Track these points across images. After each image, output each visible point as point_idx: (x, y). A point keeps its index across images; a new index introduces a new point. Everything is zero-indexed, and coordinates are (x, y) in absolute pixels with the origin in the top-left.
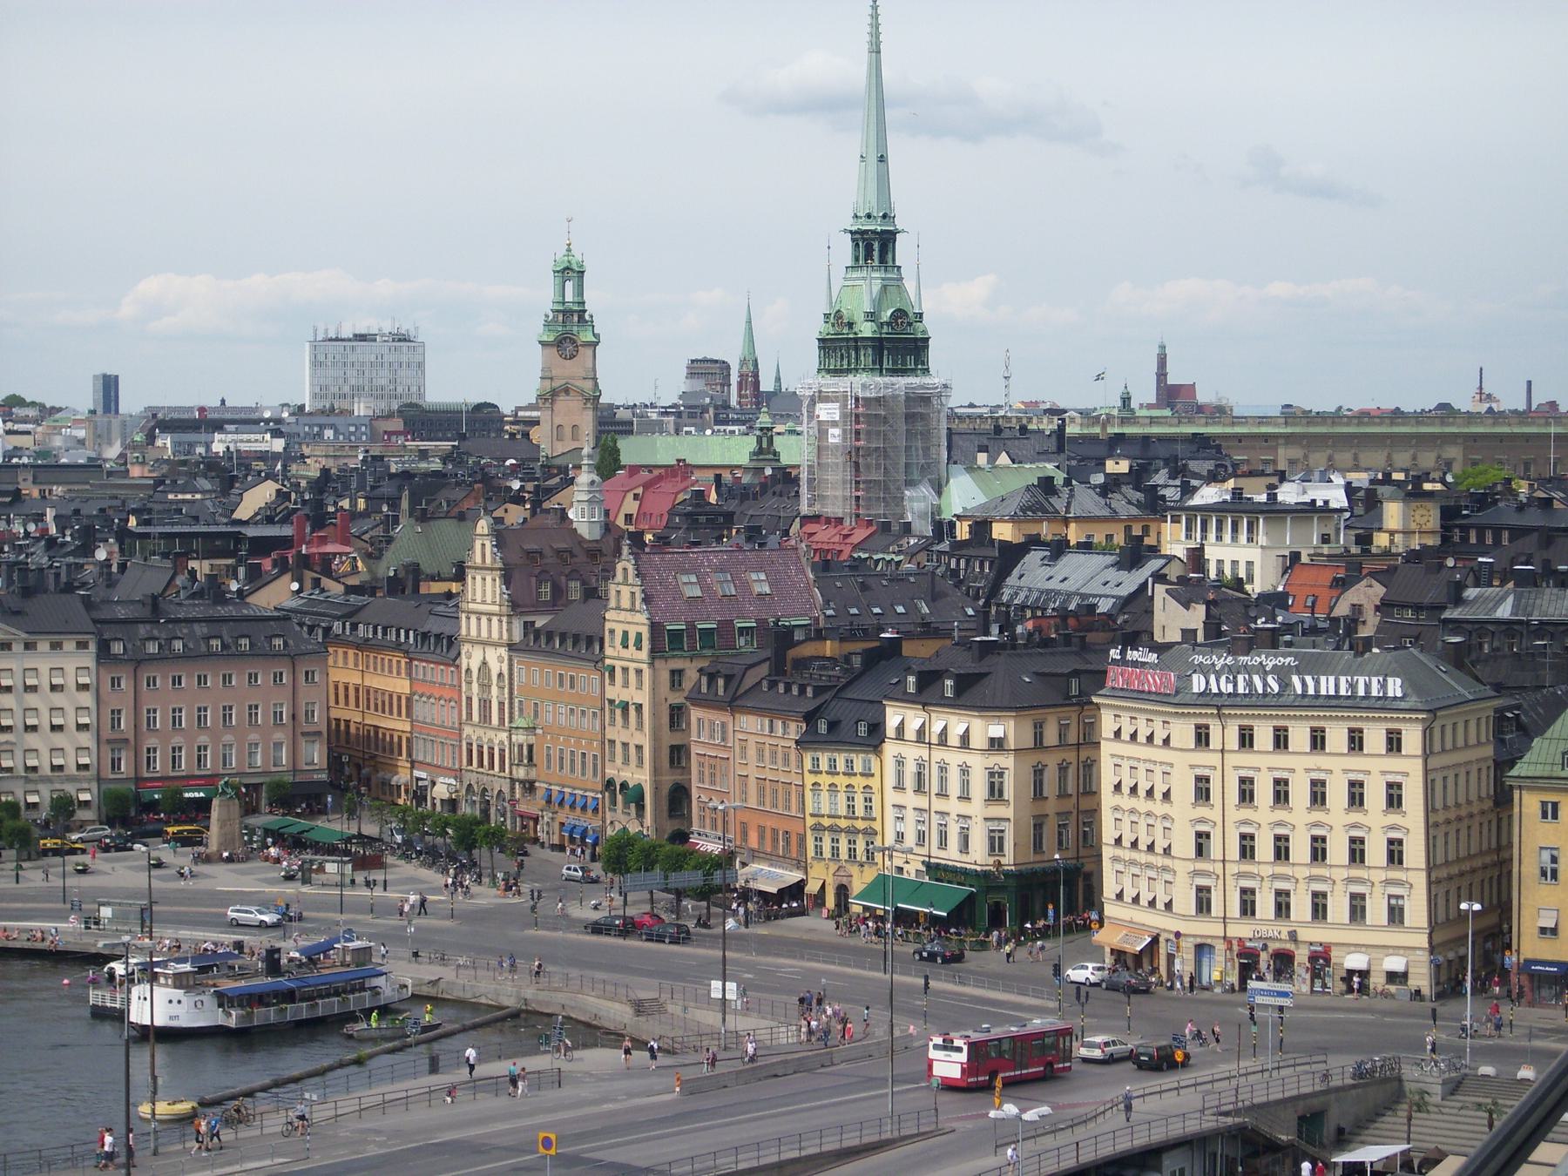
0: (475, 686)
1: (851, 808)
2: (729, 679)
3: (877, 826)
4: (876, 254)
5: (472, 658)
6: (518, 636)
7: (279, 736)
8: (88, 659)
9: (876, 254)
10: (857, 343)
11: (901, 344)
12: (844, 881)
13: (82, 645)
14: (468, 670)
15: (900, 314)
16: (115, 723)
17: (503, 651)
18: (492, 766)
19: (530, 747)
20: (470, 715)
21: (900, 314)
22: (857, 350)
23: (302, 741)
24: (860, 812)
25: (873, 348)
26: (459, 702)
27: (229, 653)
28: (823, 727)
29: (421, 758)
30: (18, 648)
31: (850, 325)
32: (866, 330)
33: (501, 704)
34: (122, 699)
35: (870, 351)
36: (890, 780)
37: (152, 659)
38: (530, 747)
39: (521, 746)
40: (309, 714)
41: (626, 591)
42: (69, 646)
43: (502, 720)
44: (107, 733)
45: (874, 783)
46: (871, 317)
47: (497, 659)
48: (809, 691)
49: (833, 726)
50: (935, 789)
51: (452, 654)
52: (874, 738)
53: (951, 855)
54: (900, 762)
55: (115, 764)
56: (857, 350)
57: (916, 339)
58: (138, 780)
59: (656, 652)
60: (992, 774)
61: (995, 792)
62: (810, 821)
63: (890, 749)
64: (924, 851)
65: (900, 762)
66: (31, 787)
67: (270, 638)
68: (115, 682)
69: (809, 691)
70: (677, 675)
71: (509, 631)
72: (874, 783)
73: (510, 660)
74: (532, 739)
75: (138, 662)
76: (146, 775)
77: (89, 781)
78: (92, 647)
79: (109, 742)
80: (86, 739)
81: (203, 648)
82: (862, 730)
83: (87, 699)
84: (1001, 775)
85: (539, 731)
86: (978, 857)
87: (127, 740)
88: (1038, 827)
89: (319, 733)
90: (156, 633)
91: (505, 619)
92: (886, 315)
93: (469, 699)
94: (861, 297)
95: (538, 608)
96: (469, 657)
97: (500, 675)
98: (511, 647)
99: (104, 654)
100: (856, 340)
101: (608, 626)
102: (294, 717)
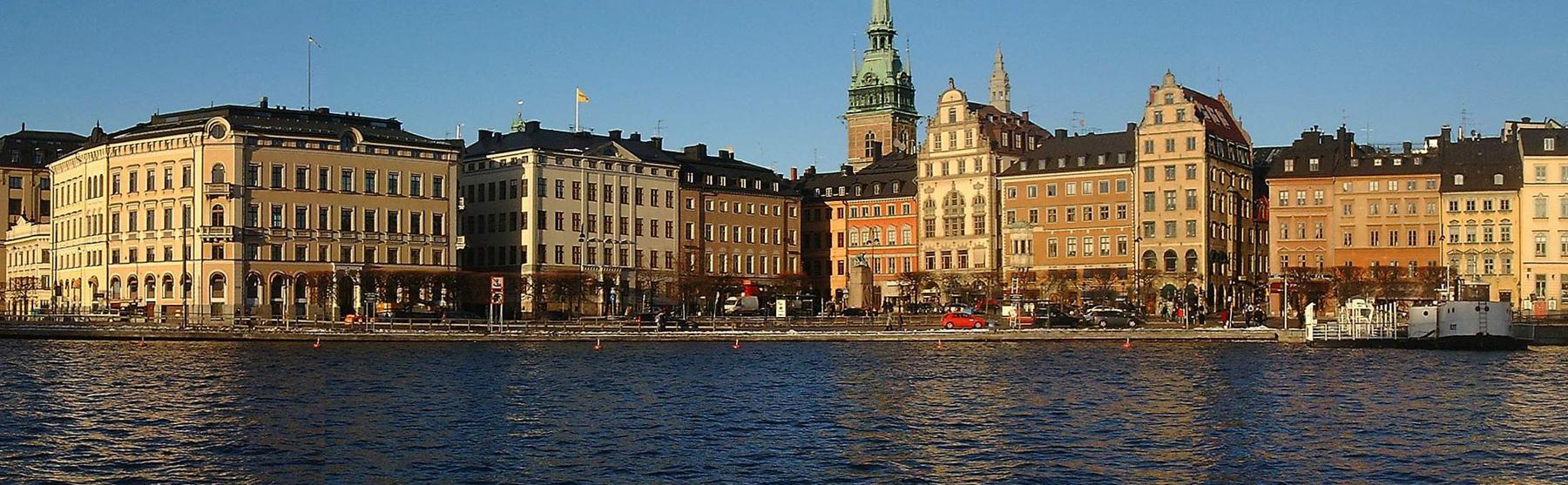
0: (939, 213)
1: (1489, 239)
3: (1514, 248)
7: (776, 252)
14: (930, 204)
17: (984, 181)
20: (930, 233)
24: (1497, 238)
28: (1459, 180)
42: (662, 172)
43: (979, 231)
45: (1512, 217)
52: (1515, 182)
54: (1541, 201)
59: (1209, 155)
65: (1541, 201)
72: (1512, 217)
82: (1499, 179)
91: (985, 159)
96: (930, 191)
97: (978, 200)
99: (682, 182)
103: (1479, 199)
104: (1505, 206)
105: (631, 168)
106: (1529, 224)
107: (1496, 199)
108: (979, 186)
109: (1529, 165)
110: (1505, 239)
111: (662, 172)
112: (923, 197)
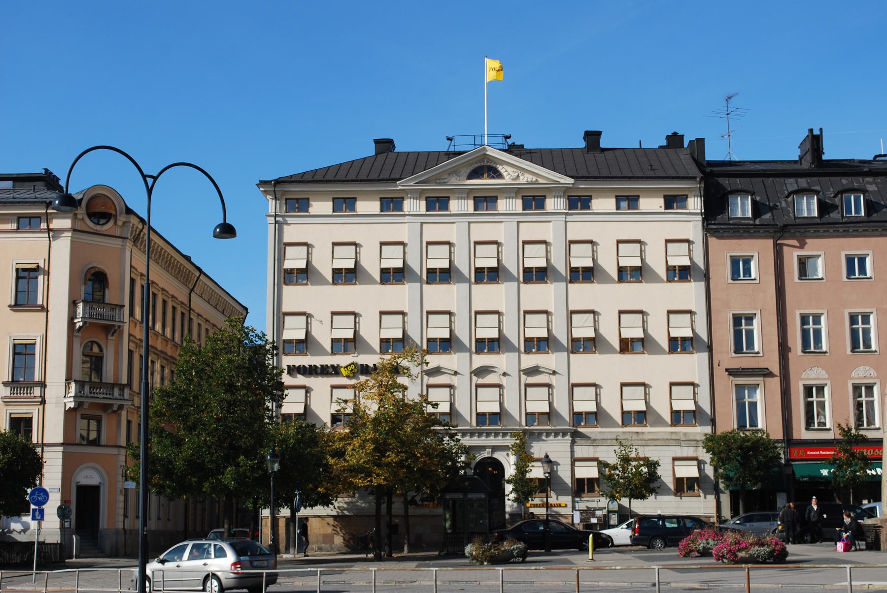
16: (741, 342)
30: (553, 204)
44: (726, 356)
58: (789, 440)
66: (582, 451)
68: (739, 267)
76: (801, 433)
78: (695, 204)
79: (732, 372)
80: (693, 365)
83: (690, 294)
87: (766, 373)
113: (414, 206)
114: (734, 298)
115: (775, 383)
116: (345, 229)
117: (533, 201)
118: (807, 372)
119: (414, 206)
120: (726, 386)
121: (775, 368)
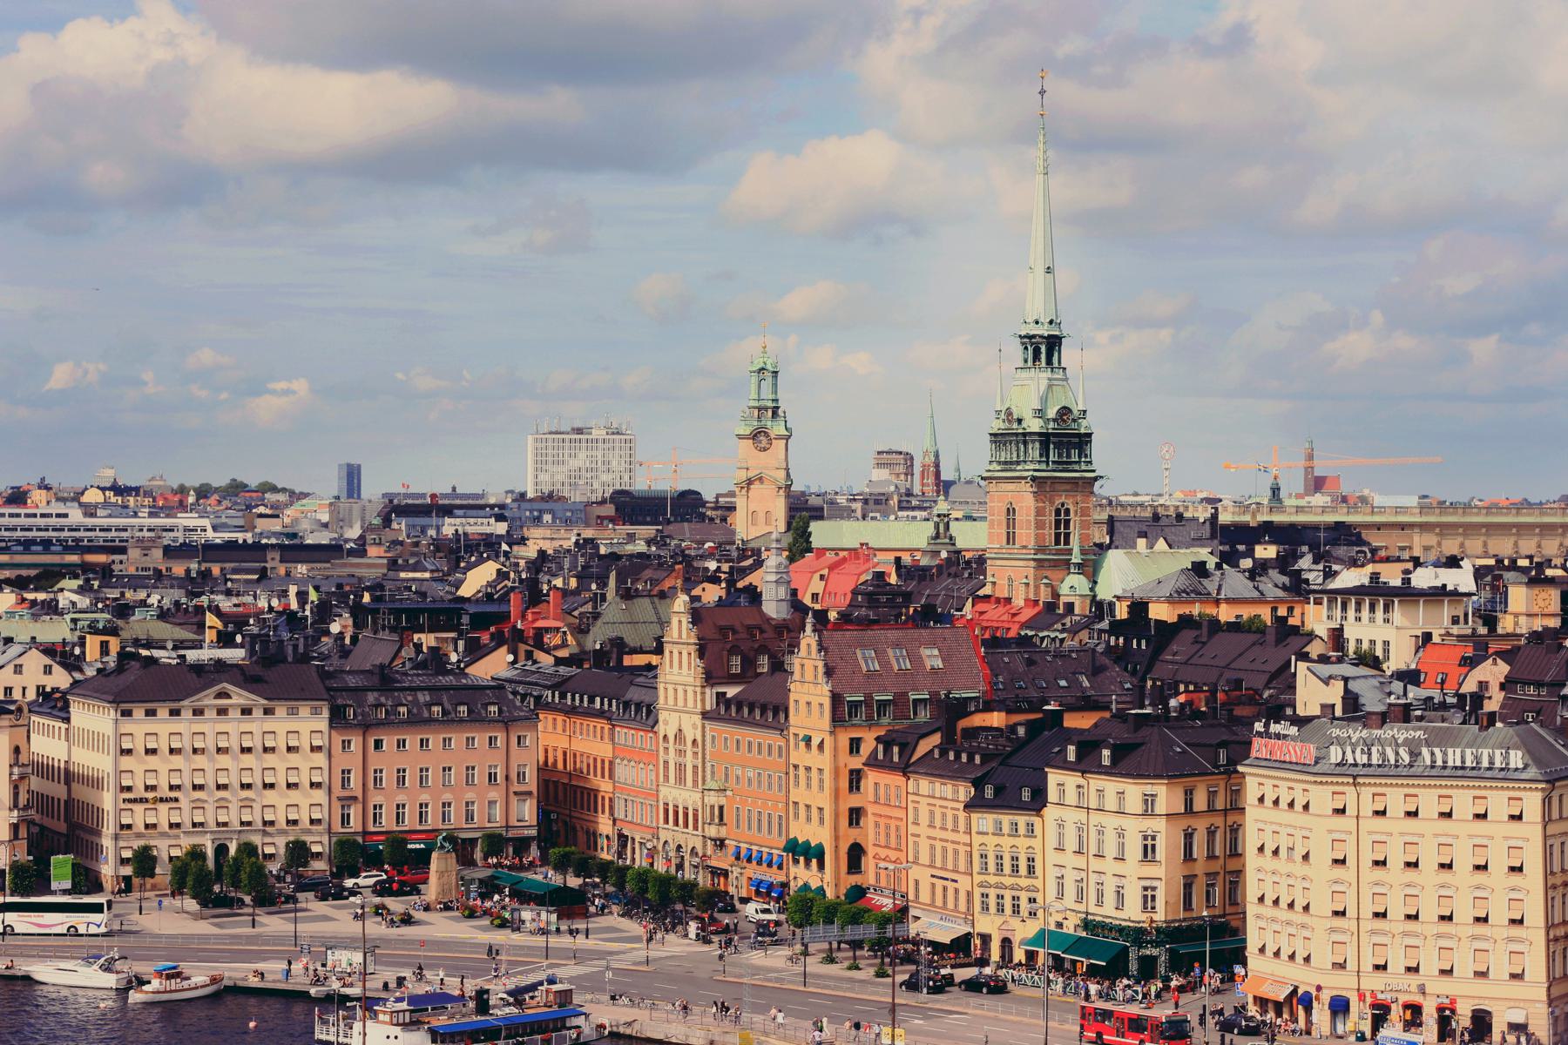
2: (903, 748)
3: (1038, 883)
4: (1043, 356)
5: (668, 722)
6: (710, 704)
7: (493, 794)
8: (322, 723)
9: (1043, 356)
10: (1025, 438)
11: (1065, 441)
12: (1008, 935)
13: (316, 711)
15: (1065, 411)
16: (345, 782)
17: (697, 719)
18: (686, 826)
19: (721, 808)
20: (666, 777)
21: (1065, 411)
22: (1025, 443)
23: (514, 800)
25: (1041, 442)
26: (656, 766)
27: (449, 720)
28: (989, 792)
29: (622, 816)
30: (258, 713)
31: (1020, 421)
32: (1034, 425)
33: (695, 767)
34: (352, 760)
35: (1037, 445)
36: (1052, 842)
37: (381, 724)
38: (721, 808)
39: (712, 807)
40: (521, 776)
41: (809, 664)
44: (338, 791)
46: (1040, 413)
47: (692, 726)
48: (978, 759)
49: (998, 791)
50: (1093, 850)
51: (650, 722)
52: (1038, 801)
53: (1106, 911)
55: (345, 819)
56: (1025, 443)
57: (1079, 435)
58: (365, 833)
59: (837, 720)
60: (1145, 838)
61: (1148, 852)
62: (978, 879)
63: (1050, 812)
64: (1082, 908)
66: (268, 840)
67: (486, 705)
68: (346, 744)
69: (978, 759)
70: (855, 745)
71: (703, 701)
72: (1036, 843)
73: (703, 727)
74: (723, 801)
75: (366, 727)
76: (372, 829)
77: (321, 834)
78: (326, 714)
79: (339, 799)
80: (320, 796)
81: (426, 714)
82: (1026, 795)
83: (320, 759)
84: (1154, 838)
85: (729, 793)
86: (1133, 913)
87: (355, 798)
88: (1188, 887)
89: (530, 793)
90: (383, 700)
92: (1052, 413)
93: (666, 763)
94: (1029, 396)
95: (732, 680)
96: (666, 722)
98: (705, 715)
99: (338, 719)
100: (1024, 435)
101: (792, 697)
102: (507, 778)
103: (1006, 819)
104: (1030, 828)
105: (258, 713)
106: (1053, 857)
107: (1022, 820)
108: (694, 726)
109: (1054, 778)
110: (1031, 870)
111: (305, 710)
112: (661, 728)
113: (187, 714)
114: (342, 761)
115: (360, 806)
116: (151, 726)
117: (246, 711)
118: (375, 798)
119: (187, 714)
120: (337, 806)
121: (360, 797)
